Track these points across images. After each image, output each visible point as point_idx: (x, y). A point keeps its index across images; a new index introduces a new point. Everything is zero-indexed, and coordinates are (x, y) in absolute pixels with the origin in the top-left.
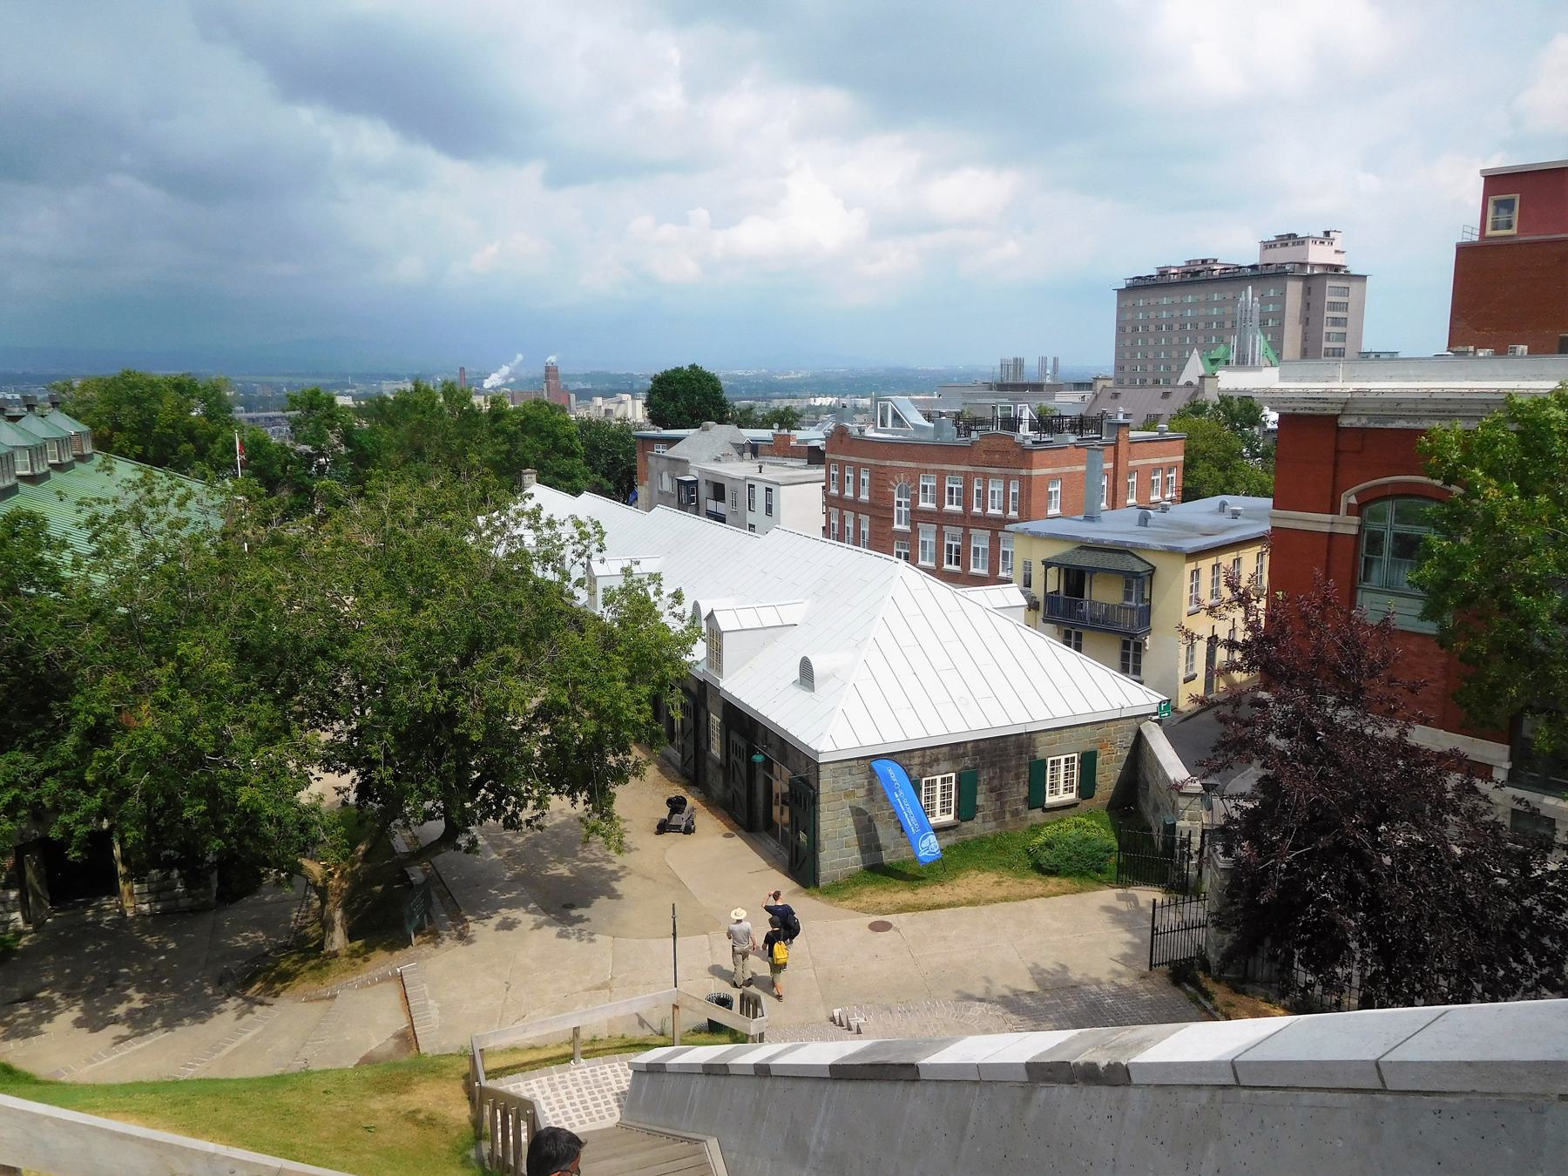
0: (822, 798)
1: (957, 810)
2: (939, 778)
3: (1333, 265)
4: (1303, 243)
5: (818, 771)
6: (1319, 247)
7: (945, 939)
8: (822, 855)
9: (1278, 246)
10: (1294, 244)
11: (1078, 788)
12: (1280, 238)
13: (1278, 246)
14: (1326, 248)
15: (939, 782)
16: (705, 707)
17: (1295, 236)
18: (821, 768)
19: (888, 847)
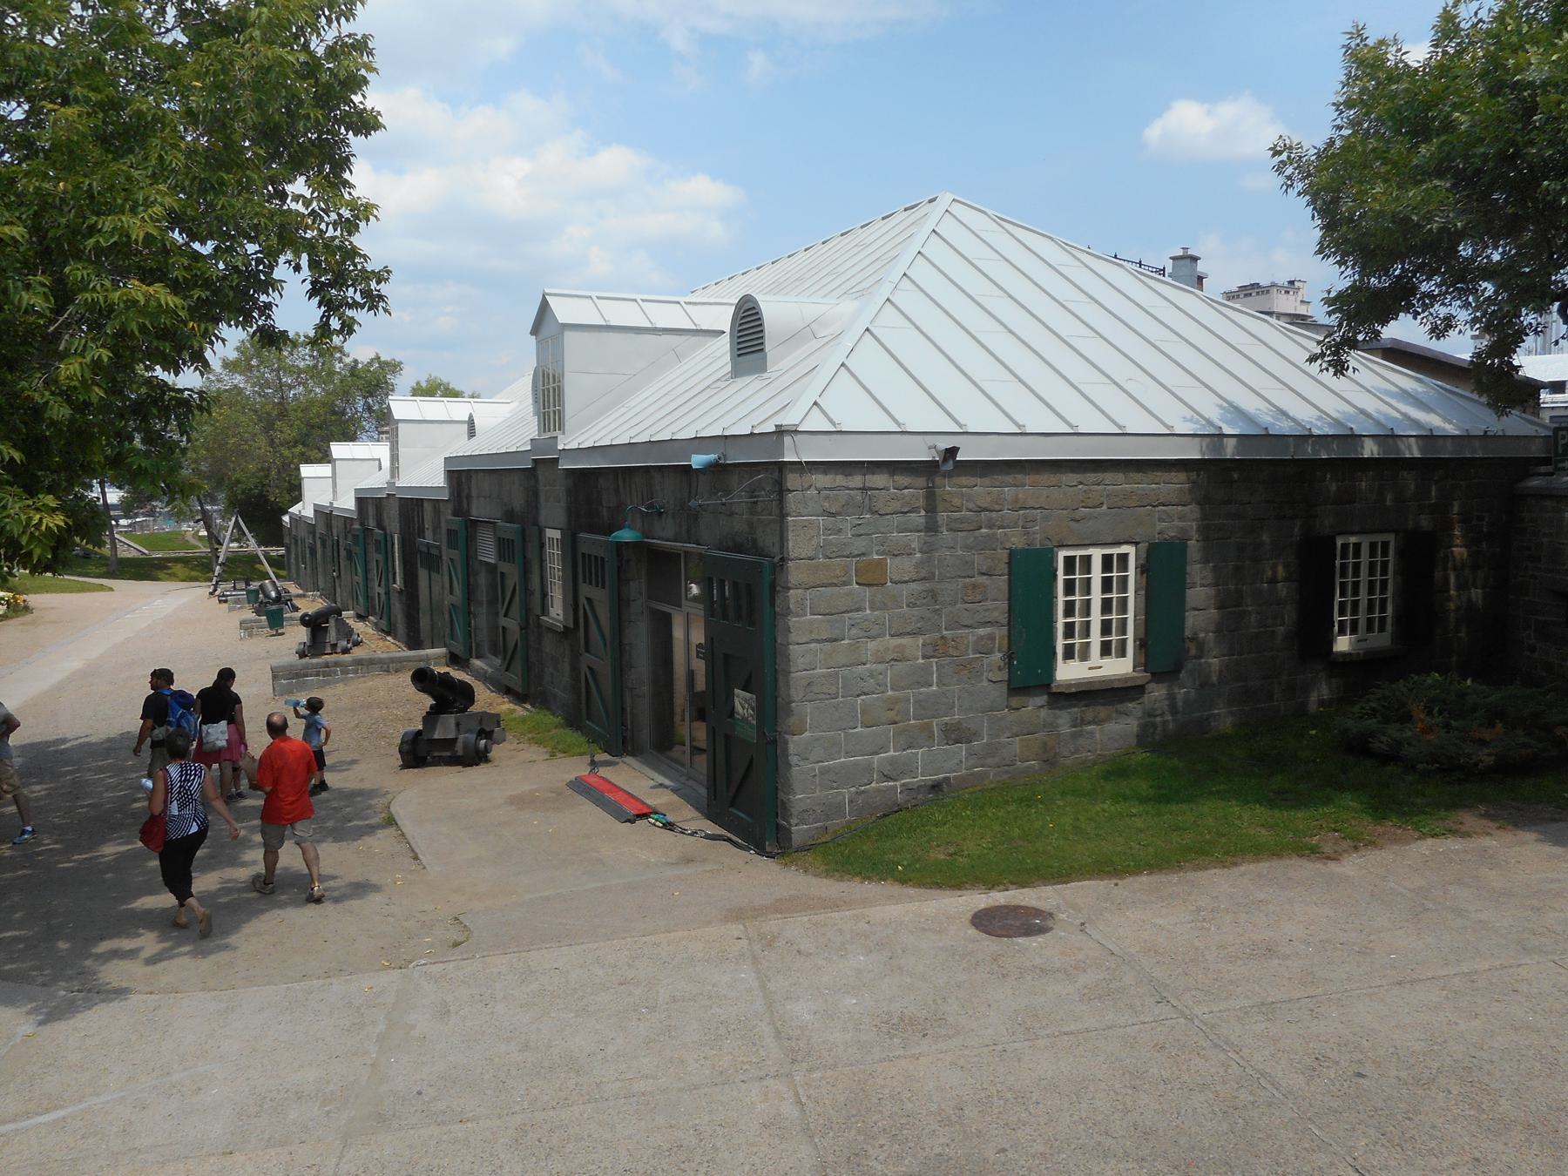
0: (796, 573)
1: (1142, 644)
2: (1097, 554)
3: (1299, 315)
4: (1268, 292)
5: (781, 491)
6: (1283, 296)
7: (1270, 951)
8: (795, 744)
9: (1242, 296)
10: (1258, 293)
11: (1398, 619)
12: (1242, 288)
13: (1242, 296)
14: (1291, 297)
15: (1097, 564)
16: (536, 522)
17: (1255, 286)
18: (792, 480)
19: (976, 735)
